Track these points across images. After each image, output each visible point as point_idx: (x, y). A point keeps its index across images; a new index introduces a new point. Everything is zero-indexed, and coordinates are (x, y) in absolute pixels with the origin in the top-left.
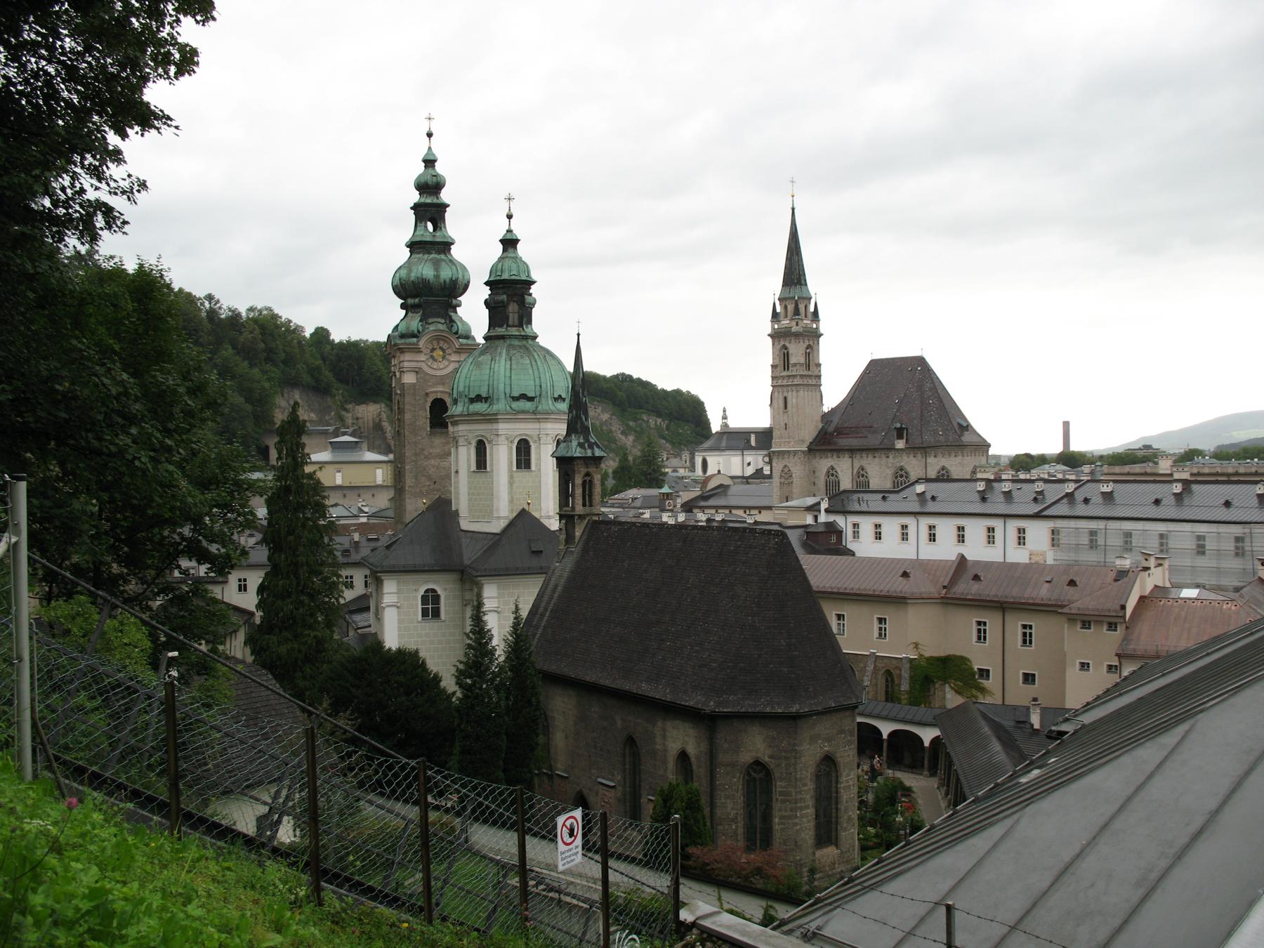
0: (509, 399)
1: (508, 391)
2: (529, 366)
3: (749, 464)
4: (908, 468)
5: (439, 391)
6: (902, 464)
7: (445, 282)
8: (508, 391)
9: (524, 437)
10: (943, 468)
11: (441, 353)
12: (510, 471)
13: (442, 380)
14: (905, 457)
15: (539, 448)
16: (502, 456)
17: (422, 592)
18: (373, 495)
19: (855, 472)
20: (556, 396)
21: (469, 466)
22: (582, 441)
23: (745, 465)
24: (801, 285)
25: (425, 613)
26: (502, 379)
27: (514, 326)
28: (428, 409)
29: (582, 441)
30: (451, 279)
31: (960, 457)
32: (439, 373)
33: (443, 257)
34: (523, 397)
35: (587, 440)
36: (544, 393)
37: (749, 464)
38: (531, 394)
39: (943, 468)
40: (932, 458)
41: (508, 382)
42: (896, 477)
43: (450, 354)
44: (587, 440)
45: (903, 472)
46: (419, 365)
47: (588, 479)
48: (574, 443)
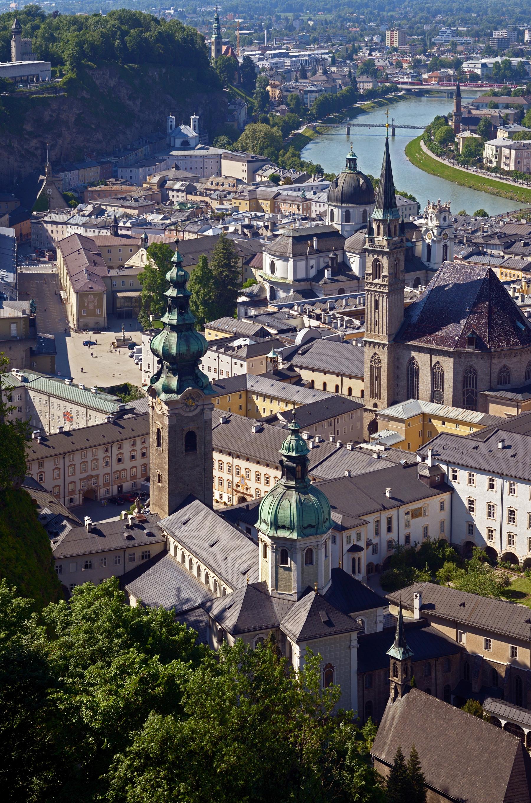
0: (302, 528)
3: (312, 267)
4: (476, 367)
5: (191, 427)
7: (193, 353)
10: (505, 366)
13: (192, 419)
14: (475, 359)
15: (317, 552)
18: (10, 348)
23: (309, 268)
24: (392, 208)
28: (184, 439)
30: (198, 351)
31: (519, 357)
32: (190, 414)
33: (190, 333)
34: (310, 526)
37: (312, 267)
38: (313, 524)
39: (505, 366)
40: (496, 359)
42: (466, 373)
45: (472, 370)
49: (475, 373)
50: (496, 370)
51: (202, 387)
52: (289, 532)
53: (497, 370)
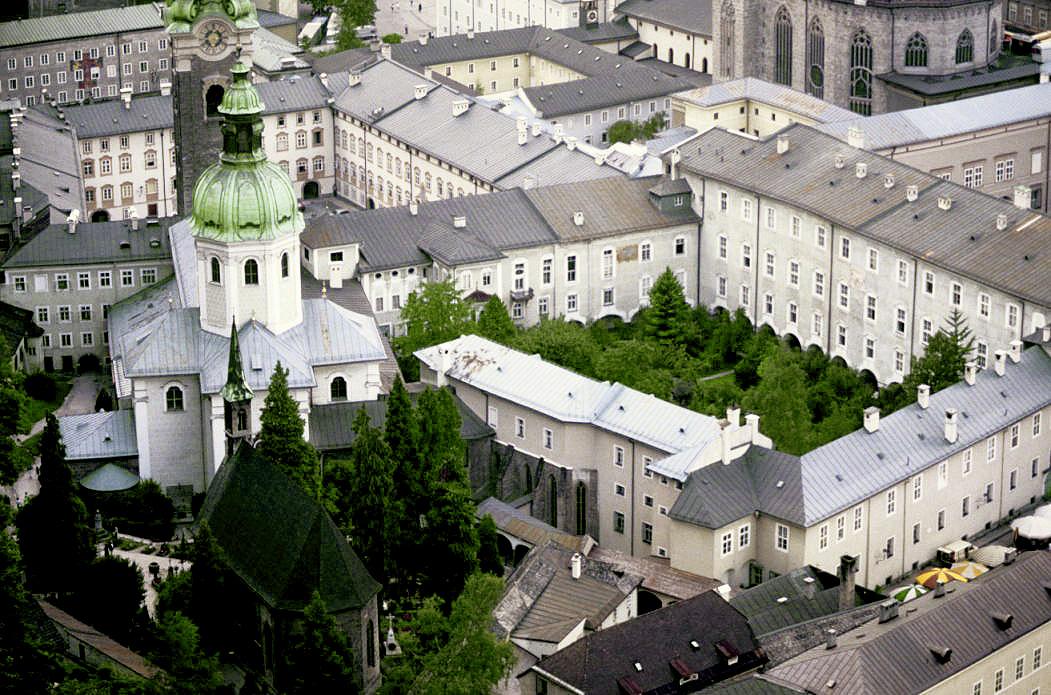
1: (236, 221)
2: (255, 197)
4: (869, 30)
6: (863, 25)
8: (236, 221)
9: (251, 258)
11: (217, 38)
12: (239, 285)
16: (234, 273)
17: (166, 389)
19: (809, 21)
20: (280, 218)
21: (206, 278)
22: (236, 389)
25: (170, 404)
26: (230, 211)
27: (244, 152)
28: (204, 96)
29: (236, 389)
34: (250, 225)
35: (240, 388)
36: (268, 220)
38: (256, 222)
40: (902, 20)
41: (235, 213)
42: (856, 41)
43: (226, 38)
44: (240, 388)
46: (195, 51)
47: (242, 412)
48: (231, 391)
49: (868, 43)
50: (902, 40)
51: (233, 15)
52: (218, 232)
53: (904, 40)
